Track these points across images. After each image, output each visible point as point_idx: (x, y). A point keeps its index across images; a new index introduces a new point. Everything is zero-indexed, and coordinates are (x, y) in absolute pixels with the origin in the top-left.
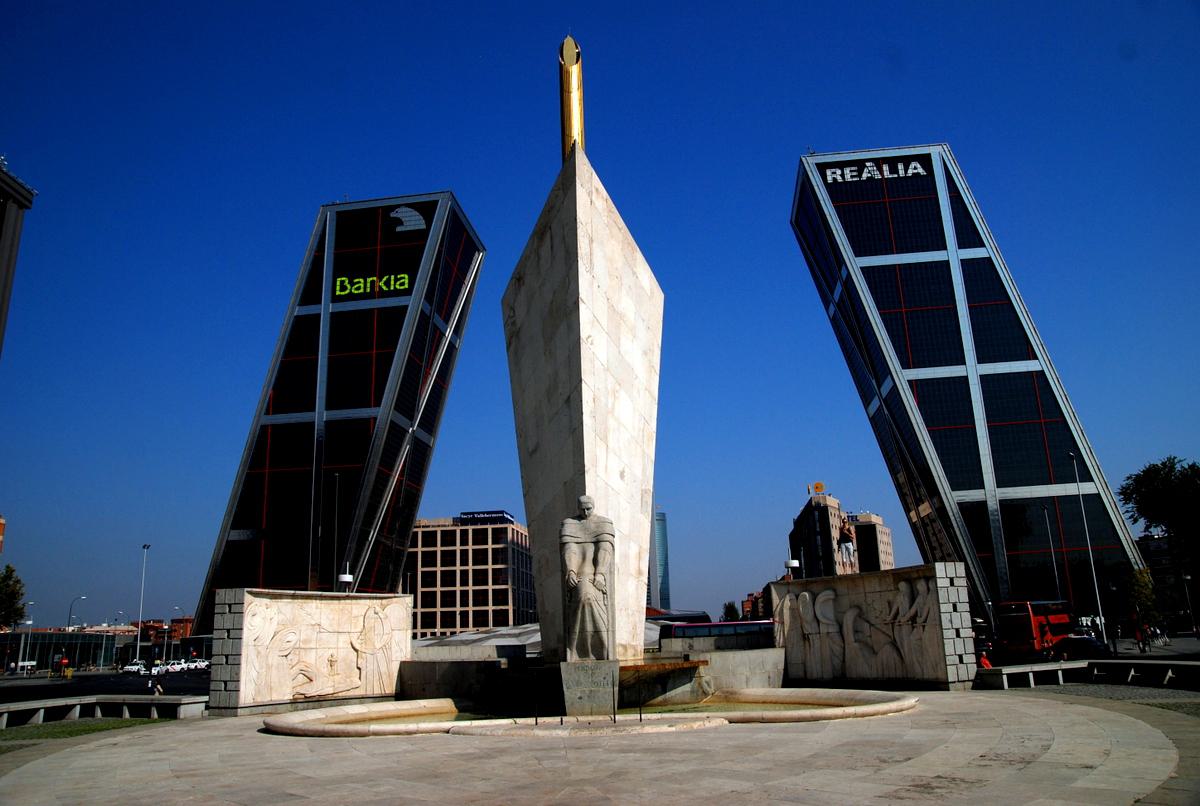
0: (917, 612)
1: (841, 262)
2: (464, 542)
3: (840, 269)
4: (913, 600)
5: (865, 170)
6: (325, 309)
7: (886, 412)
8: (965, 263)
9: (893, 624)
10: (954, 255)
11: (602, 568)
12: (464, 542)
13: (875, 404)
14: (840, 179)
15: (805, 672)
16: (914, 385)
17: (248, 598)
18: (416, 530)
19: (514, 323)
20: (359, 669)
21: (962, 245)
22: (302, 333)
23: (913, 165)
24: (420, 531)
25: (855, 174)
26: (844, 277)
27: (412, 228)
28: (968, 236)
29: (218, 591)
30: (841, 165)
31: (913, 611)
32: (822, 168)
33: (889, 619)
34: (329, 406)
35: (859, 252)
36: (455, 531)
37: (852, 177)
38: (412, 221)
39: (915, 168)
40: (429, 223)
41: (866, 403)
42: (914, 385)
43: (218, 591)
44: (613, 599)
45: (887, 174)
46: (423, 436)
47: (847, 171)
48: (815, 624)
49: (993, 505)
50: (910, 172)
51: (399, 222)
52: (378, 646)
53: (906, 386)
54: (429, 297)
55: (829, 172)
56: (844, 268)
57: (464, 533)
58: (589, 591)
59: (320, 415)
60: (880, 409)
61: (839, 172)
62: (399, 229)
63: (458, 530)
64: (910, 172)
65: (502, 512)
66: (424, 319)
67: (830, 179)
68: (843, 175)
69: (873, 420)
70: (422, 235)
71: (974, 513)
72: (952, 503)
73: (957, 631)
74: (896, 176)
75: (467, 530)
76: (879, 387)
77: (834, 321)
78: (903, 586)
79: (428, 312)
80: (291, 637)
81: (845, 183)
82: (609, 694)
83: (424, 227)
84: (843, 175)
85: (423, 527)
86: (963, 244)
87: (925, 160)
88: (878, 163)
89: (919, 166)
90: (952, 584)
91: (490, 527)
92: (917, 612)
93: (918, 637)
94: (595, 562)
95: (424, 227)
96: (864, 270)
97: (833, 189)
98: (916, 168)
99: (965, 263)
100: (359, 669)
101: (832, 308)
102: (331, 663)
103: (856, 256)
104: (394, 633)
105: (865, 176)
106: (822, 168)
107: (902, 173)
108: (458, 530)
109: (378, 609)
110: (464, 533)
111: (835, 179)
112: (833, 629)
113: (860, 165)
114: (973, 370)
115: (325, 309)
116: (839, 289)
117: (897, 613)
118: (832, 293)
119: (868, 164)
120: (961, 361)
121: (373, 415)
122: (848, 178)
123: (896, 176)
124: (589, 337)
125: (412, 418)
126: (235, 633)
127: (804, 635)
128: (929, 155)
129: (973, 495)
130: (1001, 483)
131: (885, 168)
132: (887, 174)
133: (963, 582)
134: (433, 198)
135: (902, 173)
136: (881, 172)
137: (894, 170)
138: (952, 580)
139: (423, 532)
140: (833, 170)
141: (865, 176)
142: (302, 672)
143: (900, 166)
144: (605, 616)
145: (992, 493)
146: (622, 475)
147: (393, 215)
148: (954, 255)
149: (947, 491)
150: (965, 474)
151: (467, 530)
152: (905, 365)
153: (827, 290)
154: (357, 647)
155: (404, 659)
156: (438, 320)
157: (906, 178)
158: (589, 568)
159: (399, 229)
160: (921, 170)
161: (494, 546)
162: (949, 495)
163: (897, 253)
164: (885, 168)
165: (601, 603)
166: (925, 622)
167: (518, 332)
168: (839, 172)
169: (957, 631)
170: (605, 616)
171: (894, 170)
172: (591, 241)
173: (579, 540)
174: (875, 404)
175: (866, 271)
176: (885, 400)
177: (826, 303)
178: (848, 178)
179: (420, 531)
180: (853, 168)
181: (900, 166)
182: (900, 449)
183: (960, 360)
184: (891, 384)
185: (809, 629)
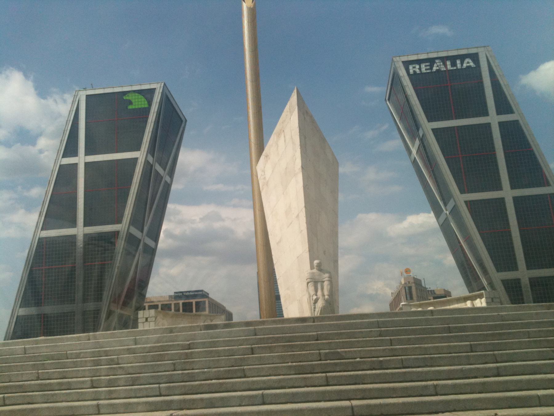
1: (417, 126)
5: (435, 65)
6: (81, 159)
8: (501, 124)
10: (493, 119)
14: (418, 71)
16: (469, 204)
18: (145, 304)
21: (499, 113)
22: (66, 175)
23: (467, 60)
25: (428, 67)
26: (421, 135)
27: (137, 107)
28: (504, 105)
30: (419, 62)
32: (407, 64)
36: (171, 304)
37: (426, 69)
38: (139, 103)
39: (468, 63)
40: (150, 103)
42: (469, 204)
45: (449, 67)
46: (151, 243)
47: (423, 66)
49: (525, 282)
50: (465, 65)
51: (130, 103)
54: (151, 150)
55: (411, 67)
56: (421, 129)
57: (177, 305)
59: (80, 230)
60: (446, 219)
61: (418, 67)
62: (130, 107)
63: (173, 303)
64: (465, 65)
65: (202, 291)
66: (148, 168)
67: (411, 72)
68: (420, 69)
70: (145, 112)
74: (455, 68)
75: (178, 303)
79: (151, 162)
81: (421, 73)
83: (146, 106)
84: (420, 69)
86: (499, 113)
87: (475, 57)
88: (444, 59)
89: (470, 61)
91: (194, 301)
95: (146, 106)
96: (434, 130)
97: (413, 78)
98: (469, 63)
99: (501, 124)
103: (429, 121)
105: (435, 69)
106: (407, 64)
107: (459, 66)
108: (173, 303)
111: (414, 72)
113: (431, 61)
114: (507, 193)
115: (81, 159)
116: (417, 142)
119: (437, 61)
122: (424, 70)
123: (455, 68)
125: (142, 232)
130: (529, 266)
131: (448, 63)
132: (449, 67)
134: (153, 86)
135: (459, 66)
137: (454, 64)
140: (414, 65)
141: (435, 69)
143: (458, 62)
145: (523, 274)
147: (125, 98)
151: (178, 303)
157: (462, 69)
159: (130, 107)
160: (472, 64)
163: (456, 119)
164: (448, 63)
168: (418, 67)
171: (454, 64)
178: (424, 70)
180: (427, 64)
181: (458, 62)
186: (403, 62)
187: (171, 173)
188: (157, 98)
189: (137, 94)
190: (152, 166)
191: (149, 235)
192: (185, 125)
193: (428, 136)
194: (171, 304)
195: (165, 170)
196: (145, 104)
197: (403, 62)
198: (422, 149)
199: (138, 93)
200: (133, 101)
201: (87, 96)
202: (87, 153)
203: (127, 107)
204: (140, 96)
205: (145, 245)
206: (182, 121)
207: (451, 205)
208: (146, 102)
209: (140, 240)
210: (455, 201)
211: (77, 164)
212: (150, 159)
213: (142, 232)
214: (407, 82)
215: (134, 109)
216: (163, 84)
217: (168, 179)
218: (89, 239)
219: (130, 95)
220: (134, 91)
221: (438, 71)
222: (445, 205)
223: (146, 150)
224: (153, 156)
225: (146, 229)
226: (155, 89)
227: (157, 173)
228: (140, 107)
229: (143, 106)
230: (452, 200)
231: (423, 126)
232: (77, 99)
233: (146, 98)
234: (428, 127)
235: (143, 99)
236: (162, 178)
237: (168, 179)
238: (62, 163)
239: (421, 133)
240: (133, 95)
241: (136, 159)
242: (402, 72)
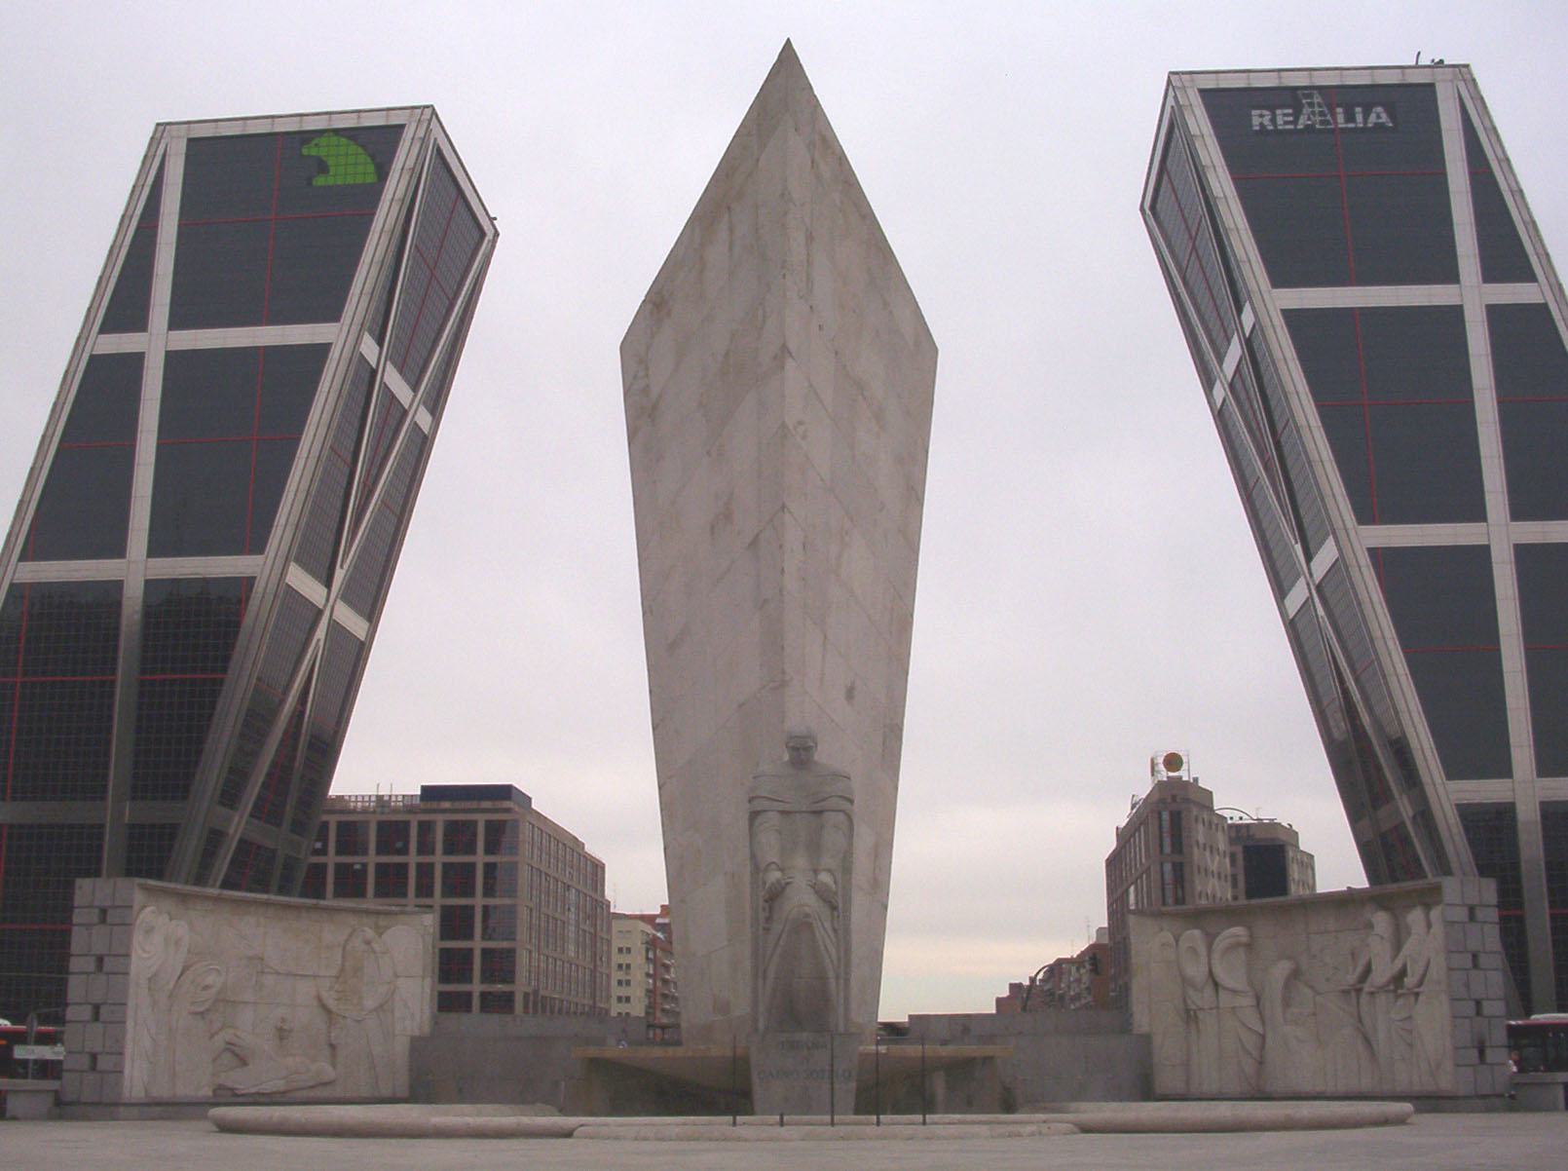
0: (1405, 966)
2: (425, 848)
3: (1239, 310)
4: (1398, 946)
7: (1321, 612)
9: (1359, 991)
10: (1473, 294)
11: (827, 861)
12: (425, 848)
13: (1298, 595)
15: (1187, 1083)
17: (139, 897)
18: (325, 818)
19: (646, 390)
20: (333, 1047)
21: (1492, 272)
24: (333, 820)
29: (79, 882)
31: (1398, 964)
33: (1351, 978)
34: (155, 549)
35: (1279, 280)
36: (407, 823)
38: (348, 168)
40: (383, 173)
41: (1280, 591)
42: (1381, 558)
43: (79, 882)
44: (847, 918)
46: (352, 621)
48: (1209, 990)
49: (1528, 814)
51: (322, 167)
52: (370, 1003)
53: (1365, 560)
56: (1247, 308)
58: (801, 898)
59: (136, 568)
60: (1308, 603)
62: (320, 181)
69: (1292, 627)
71: (1491, 828)
72: (1447, 807)
73: (1478, 1003)
76: (1309, 558)
77: (1220, 417)
78: (1381, 920)
80: (210, 980)
82: (846, 1091)
83: (371, 179)
85: (342, 812)
86: (1492, 272)
90: (1472, 917)
92: (1405, 966)
93: (1404, 1015)
94: (815, 847)
95: (371, 179)
96: (1289, 315)
100: (333, 1047)
101: (1220, 392)
102: (282, 1034)
104: (400, 982)
109: (370, 933)
110: (426, 828)
112: (1247, 1001)
115: (156, 341)
116: (1235, 351)
117: (1368, 970)
118: (1221, 362)
120: (1476, 512)
121: (248, 573)
124: (800, 423)
125: (328, 584)
126: (110, 964)
127: (1187, 1011)
128: (1432, 86)
129: (1486, 791)
133: (1493, 915)
136: (1334, 115)
138: (1472, 910)
139: (340, 824)
142: (230, 1047)
144: (833, 951)
146: (850, 693)
147: (305, 151)
148: (1473, 294)
149: (1438, 781)
150: (1475, 746)
152: (1366, 515)
153: (1211, 356)
154: (331, 1003)
155: (417, 1033)
156: (393, 380)
158: (801, 861)
159: (320, 181)
161: (491, 859)
162: (1441, 789)
165: (827, 925)
166: (1420, 983)
167: (655, 407)
169: (1478, 1003)
170: (833, 951)
172: (810, 238)
173: (787, 807)
174: (1298, 595)
175: (1292, 317)
176: (1319, 588)
177: (1208, 383)
179: (333, 820)
182: (1345, 692)
183: (1476, 512)
184: (1335, 554)
185: (1202, 998)
186: (1202, 91)
187: (436, 403)
188: (405, 156)
189: (344, 141)
190: (374, 373)
191: (349, 596)
192: (493, 247)
193: (1269, 332)
194: (407, 823)
195: (415, 388)
196: (366, 173)
197: (1202, 91)
198: (1248, 371)
199: (349, 138)
200: (331, 162)
201: (190, 141)
202: (179, 320)
203: (310, 184)
204: (353, 148)
205: (335, 627)
206: (483, 234)
207: (1326, 556)
208: (371, 168)
209: (320, 612)
210: (1340, 549)
211: (142, 355)
212: (369, 349)
213: (328, 584)
214: (1211, 153)
215: (330, 188)
216: (428, 112)
217: (424, 419)
218: (166, 599)
219: (323, 141)
220: (337, 132)
221: (1309, 129)
222: (1309, 558)
223: (358, 319)
224: (380, 342)
225: (340, 575)
226: (402, 126)
227: (390, 397)
228: (350, 180)
229: (359, 180)
230: (1330, 542)
231: (1256, 298)
232: (160, 152)
233: (373, 157)
234: (1271, 303)
235: (363, 158)
236: (405, 413)
237: (424, 419)
238: (98, 351)
239: (1248, 319)
240: (334, 139)
241: (325, 348)
242: (1199, 123)
